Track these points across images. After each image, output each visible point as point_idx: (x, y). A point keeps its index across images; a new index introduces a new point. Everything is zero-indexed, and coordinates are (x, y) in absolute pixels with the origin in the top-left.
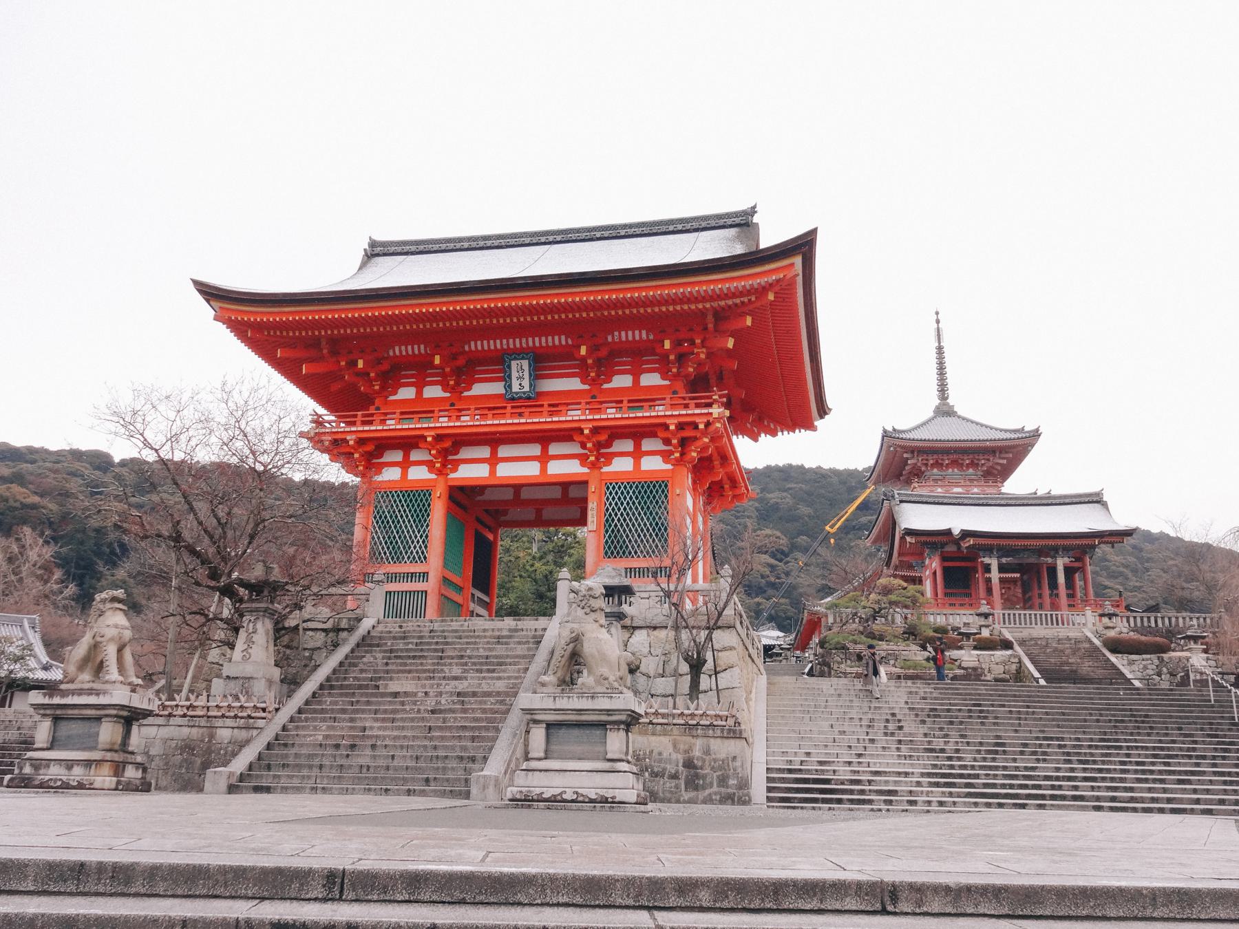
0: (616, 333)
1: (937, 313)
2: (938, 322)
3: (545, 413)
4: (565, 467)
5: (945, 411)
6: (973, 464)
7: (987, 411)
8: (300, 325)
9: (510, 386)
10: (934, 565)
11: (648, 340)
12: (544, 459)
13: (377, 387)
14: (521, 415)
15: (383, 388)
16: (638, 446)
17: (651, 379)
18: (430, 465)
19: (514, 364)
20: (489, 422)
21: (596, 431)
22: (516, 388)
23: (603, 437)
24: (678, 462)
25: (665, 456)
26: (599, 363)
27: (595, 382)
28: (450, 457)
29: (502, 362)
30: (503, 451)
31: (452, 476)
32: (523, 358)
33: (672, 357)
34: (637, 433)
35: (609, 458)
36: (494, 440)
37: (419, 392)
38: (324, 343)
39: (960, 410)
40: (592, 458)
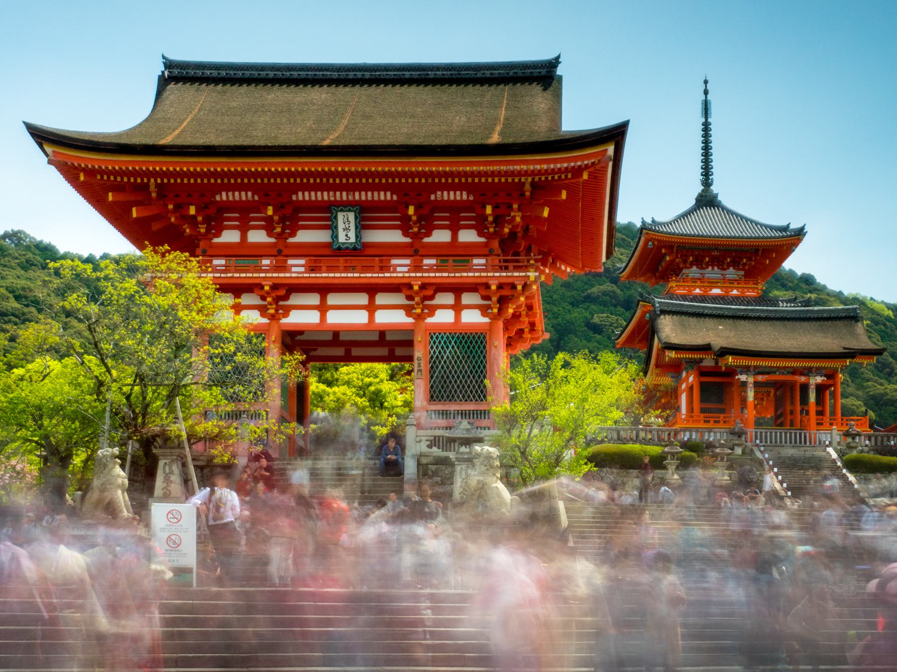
0: (439, 193)
1: (706, 82)
2: (706, 92)
3: (377, 269)
4: (392, 316)
5: (707, 201)
6: (735, 264)
7: (754, 200)
8: (135, 173)
9: (337, 237)
10: (691, 379)
11: (468, 200)
12: (371, 308)
13: (203, 231)
14: (353, 269)
15: (208, 230)
16: (458, 299)
17: (468, 236)
18: (263, 310)
19: (340, 216)
20: (324, 275)
21: (423, 287)
22: (342, 238)
23: (429, 292)
24: (494, 318)
25: (484, 310)
26: (419, 220)
27: (416, 237)
28: (281, 303)
29: (332, 213)
30: (333, 299)
31: (284, 321)
32: (350, 211)
33: (490, 219)
34: (458, 289)
35: (432, 310)
36: (324, 290)
37: (244, 236)
38: (152, 187)
39: (724, 199)
40: (419, 311)
